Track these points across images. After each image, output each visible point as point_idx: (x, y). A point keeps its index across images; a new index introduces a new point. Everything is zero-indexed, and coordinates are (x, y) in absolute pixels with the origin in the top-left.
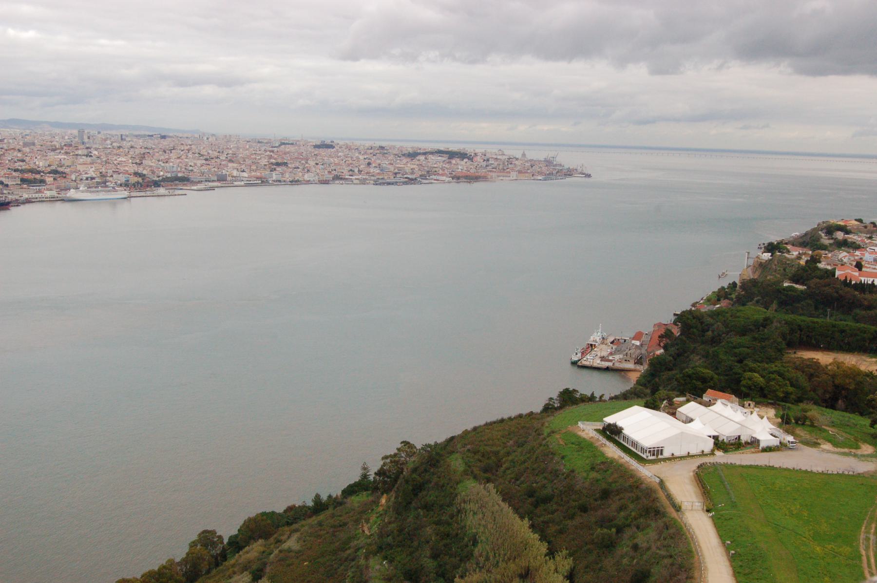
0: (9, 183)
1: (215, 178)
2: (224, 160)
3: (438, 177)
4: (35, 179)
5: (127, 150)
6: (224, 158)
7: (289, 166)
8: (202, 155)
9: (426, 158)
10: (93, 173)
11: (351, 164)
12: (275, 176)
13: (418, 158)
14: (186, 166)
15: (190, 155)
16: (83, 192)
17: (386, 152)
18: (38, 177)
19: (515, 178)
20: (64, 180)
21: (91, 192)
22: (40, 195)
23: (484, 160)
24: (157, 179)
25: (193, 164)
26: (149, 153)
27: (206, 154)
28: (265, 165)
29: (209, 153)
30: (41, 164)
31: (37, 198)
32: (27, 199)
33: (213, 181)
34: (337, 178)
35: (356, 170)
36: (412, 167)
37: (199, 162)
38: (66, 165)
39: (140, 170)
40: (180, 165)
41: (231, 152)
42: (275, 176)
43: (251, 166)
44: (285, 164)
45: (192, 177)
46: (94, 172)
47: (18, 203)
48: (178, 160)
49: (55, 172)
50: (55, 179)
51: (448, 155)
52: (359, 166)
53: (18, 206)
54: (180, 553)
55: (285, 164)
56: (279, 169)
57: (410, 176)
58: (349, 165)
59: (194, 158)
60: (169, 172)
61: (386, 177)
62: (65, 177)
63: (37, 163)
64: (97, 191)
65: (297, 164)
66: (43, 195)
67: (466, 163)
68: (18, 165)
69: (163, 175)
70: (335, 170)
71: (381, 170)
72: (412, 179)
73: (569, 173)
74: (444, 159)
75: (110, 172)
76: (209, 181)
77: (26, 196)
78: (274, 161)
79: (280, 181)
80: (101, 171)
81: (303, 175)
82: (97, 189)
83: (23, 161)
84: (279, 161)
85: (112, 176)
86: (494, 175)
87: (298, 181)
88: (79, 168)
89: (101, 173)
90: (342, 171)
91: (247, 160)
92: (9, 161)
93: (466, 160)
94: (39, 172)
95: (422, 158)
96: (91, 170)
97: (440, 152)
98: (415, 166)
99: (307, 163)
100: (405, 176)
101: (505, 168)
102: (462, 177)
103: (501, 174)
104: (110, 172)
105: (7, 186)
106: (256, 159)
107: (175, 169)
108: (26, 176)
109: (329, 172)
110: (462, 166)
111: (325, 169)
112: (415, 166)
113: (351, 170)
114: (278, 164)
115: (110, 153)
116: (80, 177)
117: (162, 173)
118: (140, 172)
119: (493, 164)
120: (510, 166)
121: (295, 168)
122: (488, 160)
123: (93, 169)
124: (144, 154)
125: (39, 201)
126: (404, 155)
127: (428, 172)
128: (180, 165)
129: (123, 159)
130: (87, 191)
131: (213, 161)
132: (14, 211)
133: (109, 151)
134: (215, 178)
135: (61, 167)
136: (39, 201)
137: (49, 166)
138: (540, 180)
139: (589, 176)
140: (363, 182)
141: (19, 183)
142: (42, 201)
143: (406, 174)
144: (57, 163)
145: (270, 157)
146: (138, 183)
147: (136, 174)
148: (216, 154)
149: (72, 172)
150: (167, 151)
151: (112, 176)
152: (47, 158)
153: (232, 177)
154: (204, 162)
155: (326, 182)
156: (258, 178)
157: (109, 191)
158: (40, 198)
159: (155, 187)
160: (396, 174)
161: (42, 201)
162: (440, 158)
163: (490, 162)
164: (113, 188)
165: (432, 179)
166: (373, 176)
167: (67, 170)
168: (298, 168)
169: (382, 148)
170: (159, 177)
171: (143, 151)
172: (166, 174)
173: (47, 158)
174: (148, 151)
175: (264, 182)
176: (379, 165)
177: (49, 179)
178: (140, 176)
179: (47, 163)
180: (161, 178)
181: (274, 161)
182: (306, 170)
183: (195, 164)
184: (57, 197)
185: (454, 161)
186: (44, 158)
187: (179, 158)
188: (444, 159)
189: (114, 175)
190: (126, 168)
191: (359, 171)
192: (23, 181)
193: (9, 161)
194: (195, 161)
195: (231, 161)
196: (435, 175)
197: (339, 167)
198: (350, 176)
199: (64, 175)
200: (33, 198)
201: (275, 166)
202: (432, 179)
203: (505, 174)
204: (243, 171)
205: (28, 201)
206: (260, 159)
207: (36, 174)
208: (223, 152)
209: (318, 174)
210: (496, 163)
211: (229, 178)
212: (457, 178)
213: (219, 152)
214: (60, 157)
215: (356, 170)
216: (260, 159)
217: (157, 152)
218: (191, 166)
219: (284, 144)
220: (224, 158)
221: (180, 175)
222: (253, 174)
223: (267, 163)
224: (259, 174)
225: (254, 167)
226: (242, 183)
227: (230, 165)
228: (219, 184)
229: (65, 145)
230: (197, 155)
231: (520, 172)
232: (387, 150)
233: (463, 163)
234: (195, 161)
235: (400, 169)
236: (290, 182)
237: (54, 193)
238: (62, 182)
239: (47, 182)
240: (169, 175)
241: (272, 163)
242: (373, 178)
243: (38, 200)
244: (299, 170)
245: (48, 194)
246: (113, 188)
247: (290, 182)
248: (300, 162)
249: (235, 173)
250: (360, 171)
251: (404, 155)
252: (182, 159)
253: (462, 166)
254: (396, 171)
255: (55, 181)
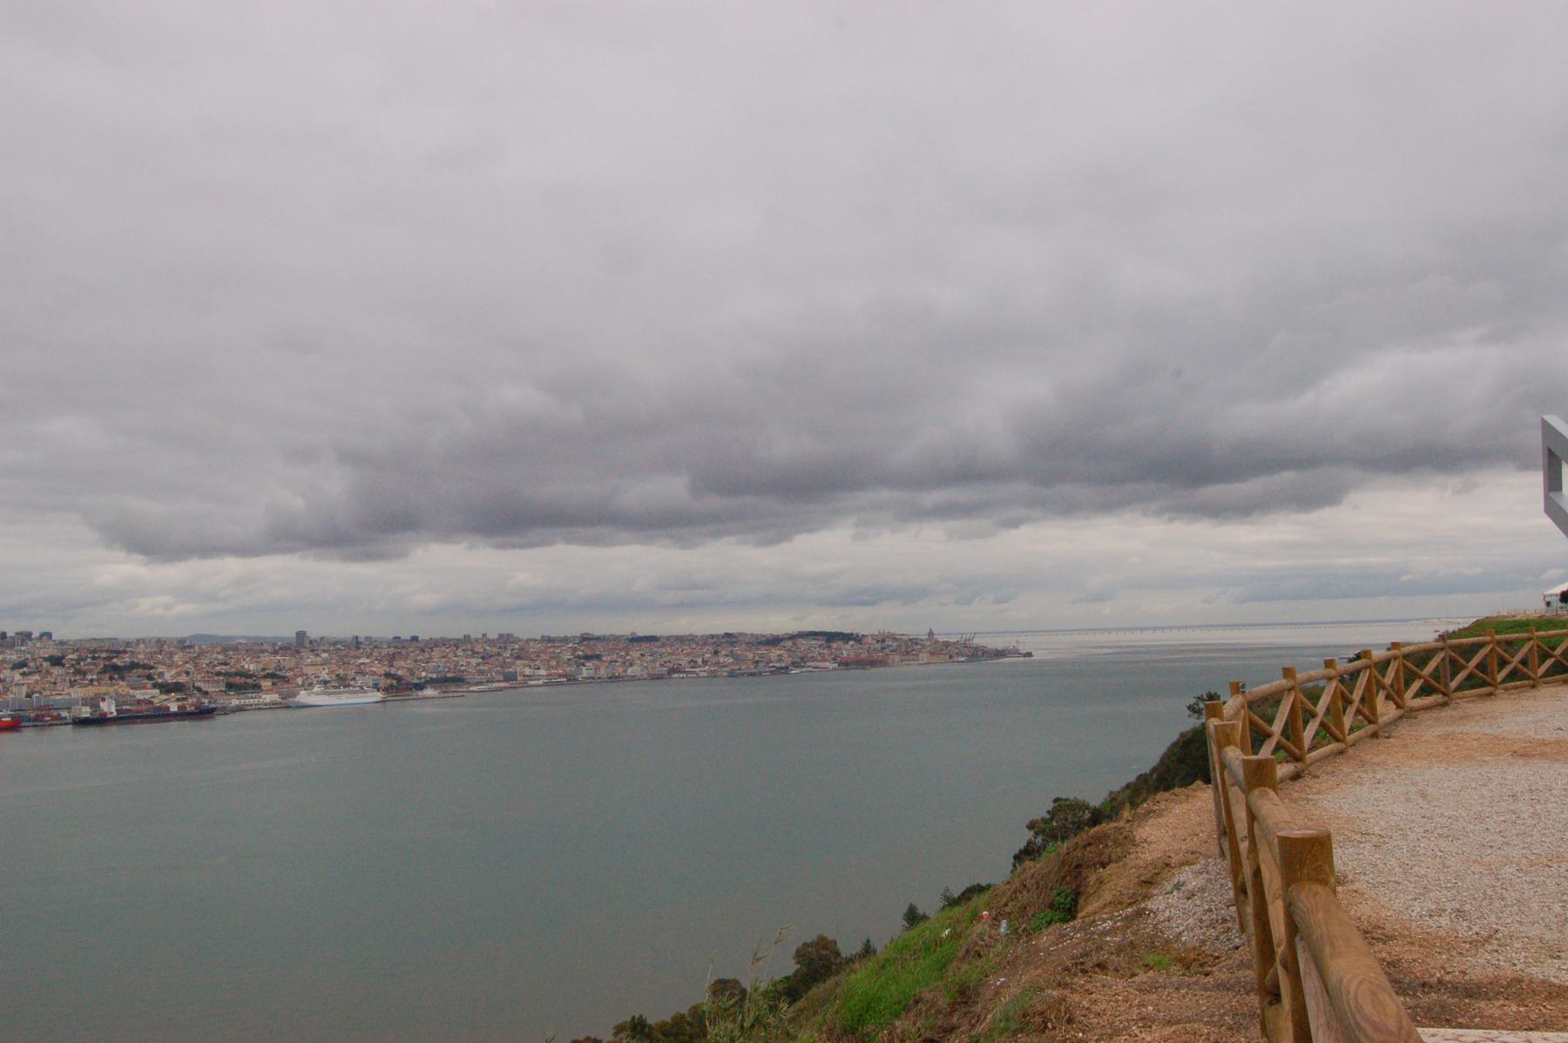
0: (210, 690)
1: (501, 678)
2: (508, 658)
3: (818, 664)
4: (245, 683)
5: (369, 651)
6: (508, 655)
7: (604, 659)
8: (477, 653)
9: (794, 644)
10: (326, 676)
11: (692, 653)
12: (585, 672)
13: (782, 644)
14: (456, 666)
15: (460, 653)
16: (317, 694)
17: (734, 640)
18: (250, 681)
19: (925, 661)
20: (286, 686)
21: (329, 694)
22: (256, 700)
23: (878, 641)
24: (418, 681)
25: (465, 663)
26: (400, 653)
27: (482, 650)
28: (569, 660)
29: (485, 650)
30: (252, 667)
31: (251, 705)
32: (237, 706)
33: (499, 681)
34: (672, 671)
35: (700, 661)
36: (779, 652)
37: (474, 661)
38: (287, 667)
39: (393, 671)
40: (448, 664)
41: (517, 646)
42: (585, 672)
43: (549, 661)
44: (598, 657)
45: (468, 677)
46: (328, 674)
47: (227, 711)
48: (443, 660)
49: (273, 676)
50: (274, 684)
51: (825, 638)
52: (703, 655)
53: (225, 714)
54: (668, 1020)
55: (598, 657)
56: (589, 664)
57: (778, 665)
58: (688, 655)
59: (467, 657)
60: (434, 672)
61: (743, 667)
62: (288, 682)
63: (246, 667)
64: (339, 693)
65: (615, 657)
66: (261, 700)
67: (852, 646)
68: (223, 668)
69: (425, 677)
70: (669, 662)
71: (736, 659)
72: (781, 668)
73: (1000, 654)
74: (820, 643)
75: (351, 673)
76: (493, 682)
77: (235, 702)
78: (581, 653)
79: (593, 678)
80: (337, 673)
81: (625, 671)
82: (338, 690)
83: (226, 664)
84: (589, 653)
85: (354, 679)
86: (897, 658)
87: (619, 677)
88: (306, 670)
89: (338, 675)
90: (680, 662)
91: (542, 655)
92: (207, 665)
93: (851, 643)
94: (251, 676)
95: (789, 644)
96: (324, 672)
97: (814, 635)
98: (782, 652)
99: (627, 654)
100: (771, 665)
101: (909, 650)
102: (852, 662)
103: (907, 657)
104: (351, 673)
105: (206, 693)
106: (554, 652)
107: (441, 669)
108: (232, 680)
109: (662, 665)
110: (847, 650)
111: (654, 661)
112: (782, 652)
113: (692, 661)
114: (587, 658)
115: (346, 656)
116: (310, 681)
117: (424, 674)
118: (392, 672)
119: (891, 646)
120: (915, 647)
121: (612, 662)
122: (883, 641)
123: (327, 671)
124: (395, 654)
125: (255, 709)
126: (760, 643)
127: (802, 658)
128: (448, 664)
129: (367, 661)
130: (323, 693)
131: (493, 659)
132: (220, 720)
133: (344, 653)
134: (501, 678)
135: (280, 670)
136: (255, 709)
137: (263, 670)
138: (963, 662)
139: (1029, 654)
140: (713, 675)
141: (224, 689)
142: (259, 709)
143: (772, 662)
144: (274, 666)
145: (574, 650)
146: (392, 686)
147: (387, 675)
148: (495, 650)
149: (296, 676)
150: (427, 650)
151: (354, 679)
152: (260, 660)
153: (524, 676)
154: (480, 660)
155: (660, 677)
156: (561, 676)
157: (356, 692)
158: (256, 705)
159: (416, 690)
160: (757, 662)
161: (259, 709)
162: (813, 642)
163: (887, 643)
164: (361, 688)
165: (809, 667)
166: (725, 666)
167: (289, 674)
168: (616, 661)
169: (728, 635)
170: (420, 678)
171: (392, 650)
172: (430, 675)
173: (260, 660)
174: (399, 650)
175: (571, 679)
176: (732, 651)
177: (266, 684)
178: (394, 679)
179: (261, 666)
180: (422, 681)
181: (581, 653)
182: (628, 664)
183: (469, 663)
184: (281, 703)
185: (835, 645)
186: (256, 660)
187: (443, 657)
188: (820, 643)
189: (357, 678)
190: (374, 669)
191: (703, 661)
192: (230, 686)
193: (207, 665)
194: (468, 660)
195: (518, 657)
196: (813, 661)
197: (674, 657)
198: (692, 667)
199: (286, 680)
200: (247, 705)
201: (583, 661)
202: (809, 667)
203: (911, 657)
204: (539, 669)
205: (240, 709)
206: (561, 652)
207: (247, 678)
208: (505, 648)
209: (646, 668)
210: (895, 644)
211: (519, 678)
212: (845, 664)
213: (500, 648)
214: (278, 657)
215: (700, 661)
216: (561, 652)
217: (412, 652)
218: (462, 665)
219: (588, 639)
220: (508, 655)
221: (449, 675)
222: (553, 671)
223: (572, 657)
224: (561, 671)
225: (554, 663)
226: (541, 682)
227: (518, 662)
228: (503, 684)
229: (281, 649)
230: (470, 653)
231: (932, 654)
232: (736, 637)
233: (848, 646)
234: (468, 660)
235: (761, 656)
236: (608, 678)
237: (276, 697)
238: (286, 688)
239: (263, 688)
240: (435, 676)
241: (579, 657)
242: (725, 669)
243: (253, 707)
244: (618, 664)
245: (268, 698)
246: (361, 688)
247: (608, 678)
248: (618, 654)
249: (528, 671)
250: (705, 662)
251: (760, 643)
252: (449, 658)
253: (847, 650)
254: (757, 658)
255: (274, 687)
